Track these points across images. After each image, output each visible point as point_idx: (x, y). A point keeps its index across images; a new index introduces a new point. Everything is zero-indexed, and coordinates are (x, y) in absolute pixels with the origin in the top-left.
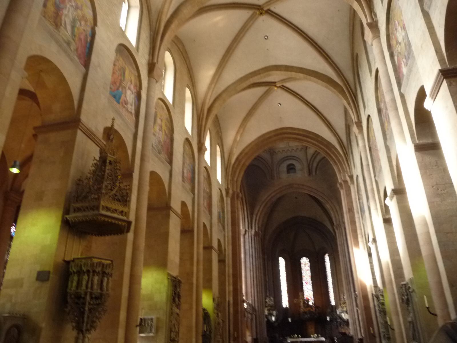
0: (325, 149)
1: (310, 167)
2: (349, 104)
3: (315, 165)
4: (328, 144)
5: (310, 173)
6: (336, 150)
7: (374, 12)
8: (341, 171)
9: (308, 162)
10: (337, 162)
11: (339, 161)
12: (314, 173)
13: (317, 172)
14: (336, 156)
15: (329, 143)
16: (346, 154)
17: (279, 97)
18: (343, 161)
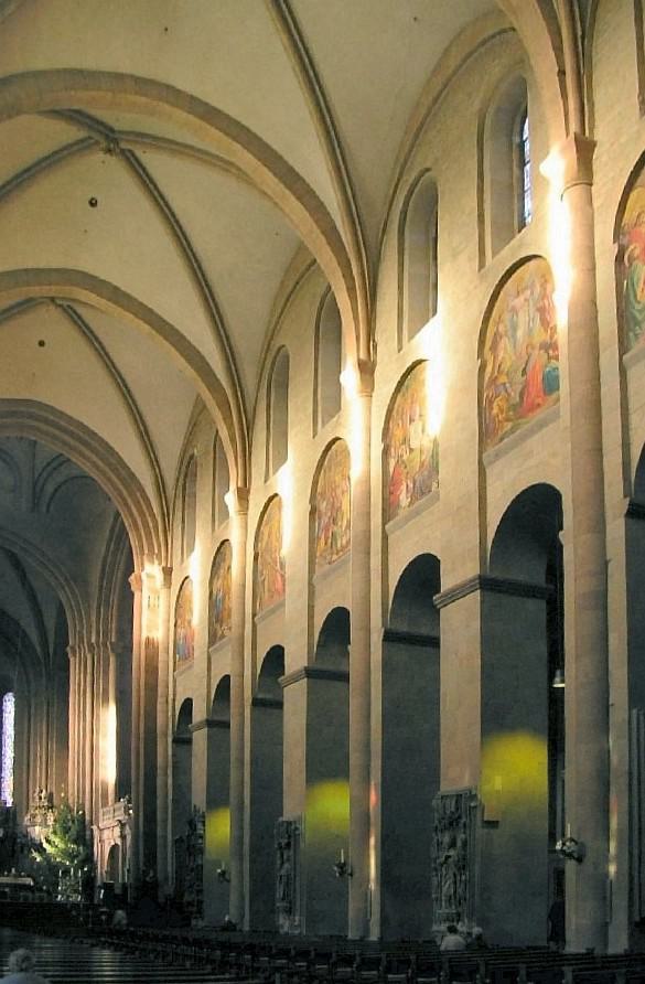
0: (121, 487)
1: (38, 489)
2: (233, 440)
3: (50, 488)
4: (130, 479)
5: (35, 505)
6: (143, 491)
7: (374, 341)
8: (146, 552)
9: (34, 474)
10: (140, 523)
11: (146, 525)
12: (44, 509)
13: (52, 508)
14: (142, 514)
15: (132, 476)
16: (166, 516)
17: (51, 325)
18: (156, 527)
